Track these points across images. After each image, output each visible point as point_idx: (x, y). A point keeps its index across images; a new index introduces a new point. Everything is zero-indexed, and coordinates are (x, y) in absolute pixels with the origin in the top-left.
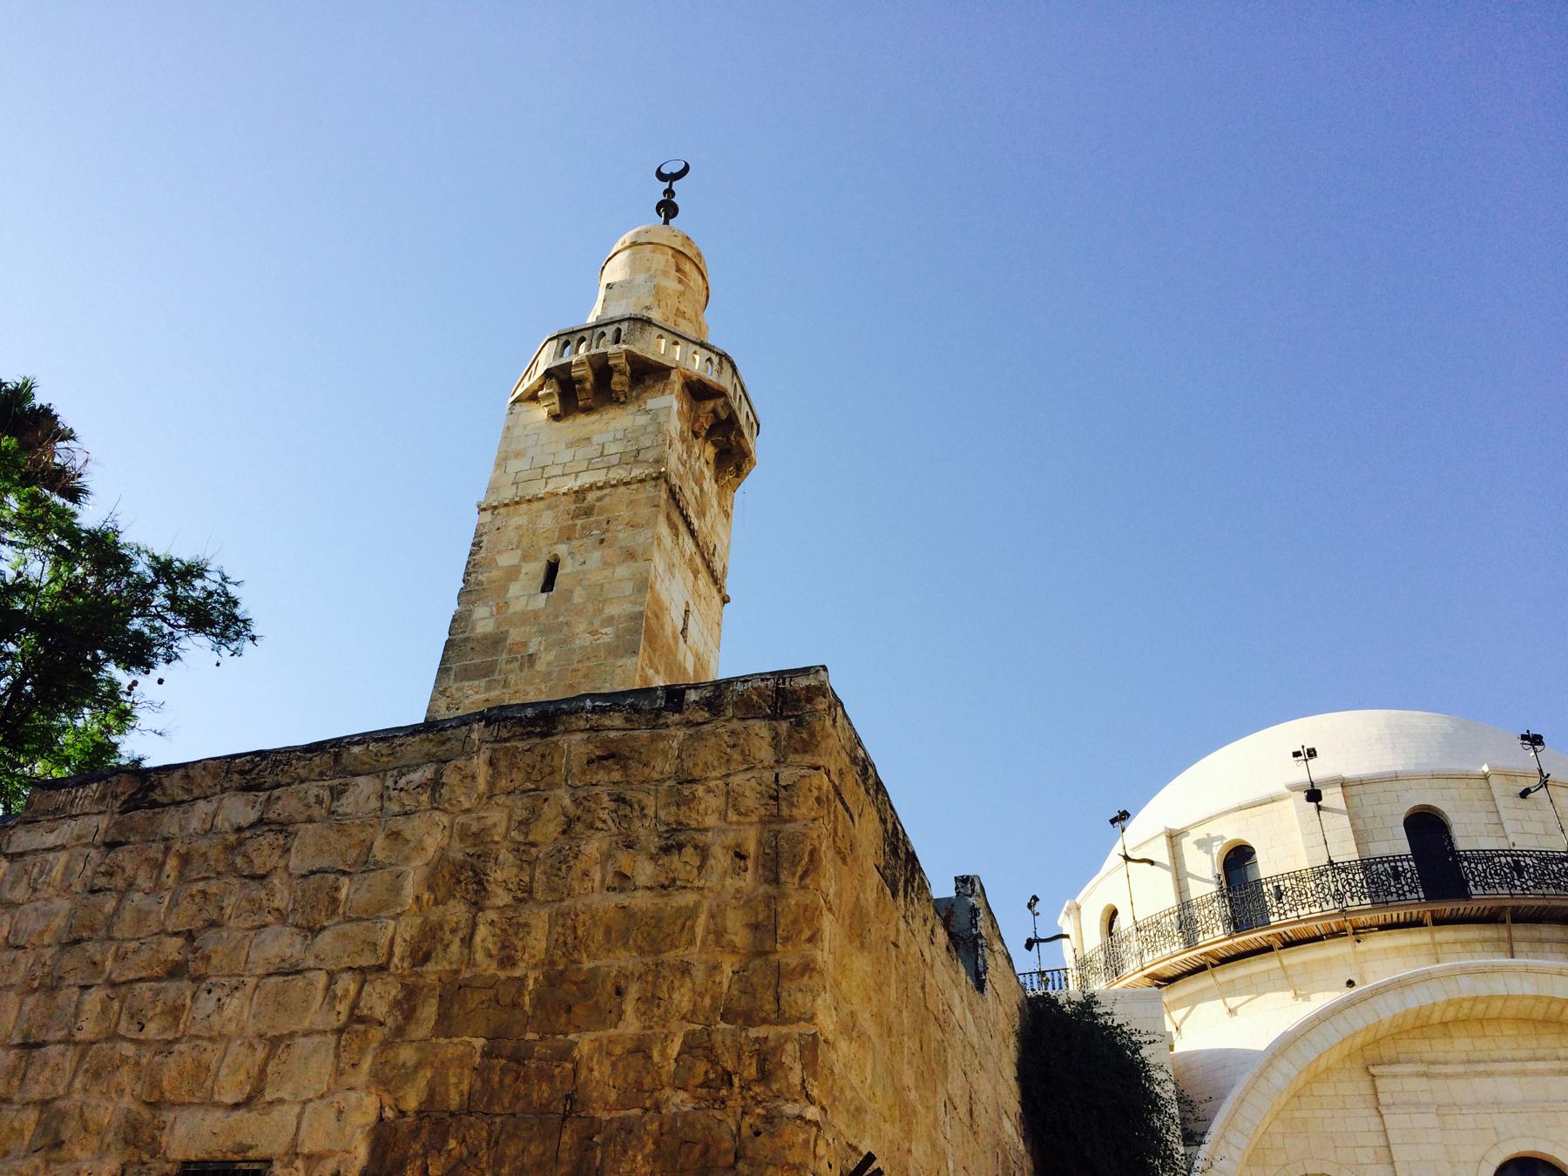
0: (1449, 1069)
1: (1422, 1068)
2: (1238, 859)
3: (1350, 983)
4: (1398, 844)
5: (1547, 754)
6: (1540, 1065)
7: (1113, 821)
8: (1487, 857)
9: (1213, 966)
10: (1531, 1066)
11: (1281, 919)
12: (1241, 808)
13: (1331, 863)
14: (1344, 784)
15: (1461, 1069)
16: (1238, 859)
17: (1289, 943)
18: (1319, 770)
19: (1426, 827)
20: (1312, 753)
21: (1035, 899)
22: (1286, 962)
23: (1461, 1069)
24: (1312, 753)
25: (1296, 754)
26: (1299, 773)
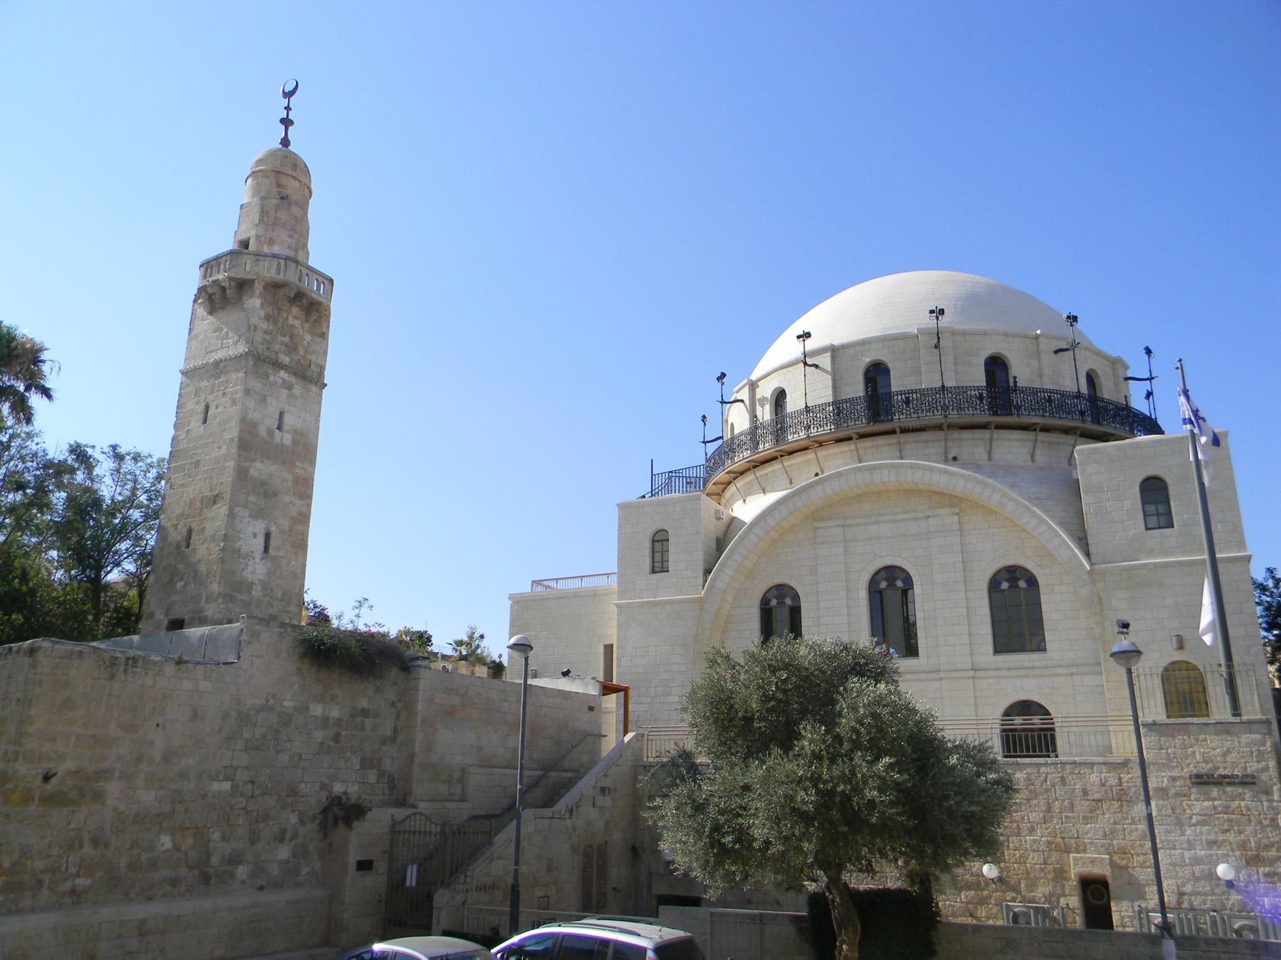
0: (857, 521)
2: (780, 396)
4: (856, 389)
5: (944, 321)
6: (905, 516)
9: (755, 467)
10: (899, 517)
11: (795, 437)
14: (834, 351)
15: (863, 521)
16: (780, 396)
17: (791, 453)
18: (811, 344)
19: (876, 374)
20: (807, 335)
21: (704, 417)
23: (863, 521)
24: (808, 335)
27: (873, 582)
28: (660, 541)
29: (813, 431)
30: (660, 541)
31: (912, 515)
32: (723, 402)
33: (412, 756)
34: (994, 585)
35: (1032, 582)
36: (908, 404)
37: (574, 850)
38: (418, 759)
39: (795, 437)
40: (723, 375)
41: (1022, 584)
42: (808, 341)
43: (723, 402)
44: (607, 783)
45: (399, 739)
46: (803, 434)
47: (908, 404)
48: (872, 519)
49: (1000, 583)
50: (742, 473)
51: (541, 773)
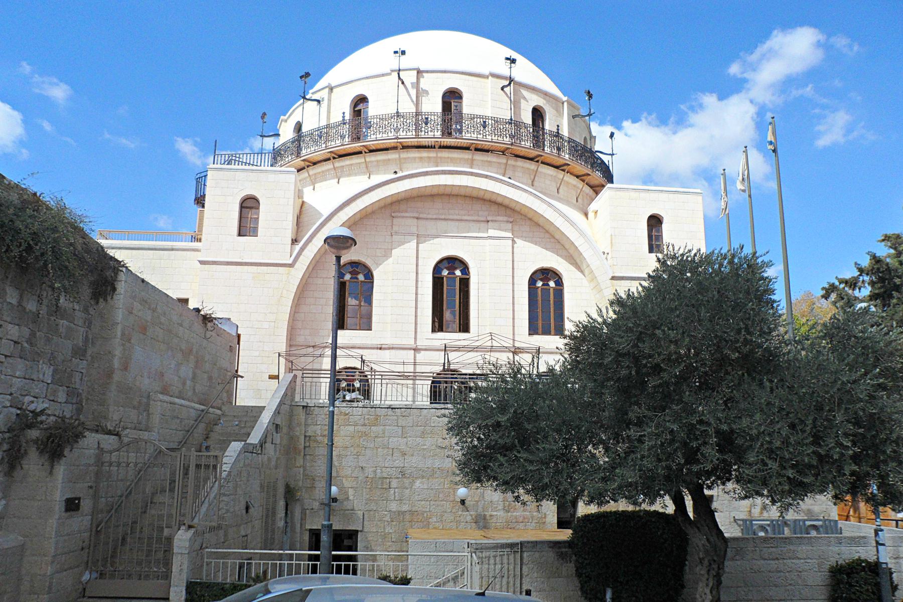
1: (416, 215)
3: (396, 172)
7: (301, 77)
8: (472, 117)
9: (334, 158)
12: (367, 78)
13: (397, 112)
15: (434, 217)
18: (405, 62)
19: (452, 97)
21: (264, 114)
22: (368, 160)
25: (396, 52)
26: (394, 62)
27: (437, 269)
28: (249, 205)
29: (402, 134)
30: (249, 205)
31: (476, 218)
32: (304, 98)
33: (109, 374)
34: (532, 281)
35: (559, 282)
36: (484, 127)
37: (262, 486)
38: (117, 377)
39: (374, 138)
40: (307, 75)
41: (552, 284)
42: (403, 57)
43: (304, 98)
44: (278, 421)
45: (89, 352)
46: (391, 135)
47: (484, 127)
48: (443, 217)
49: (536, 281)
50: (314, 164)
51: (203, 407)
